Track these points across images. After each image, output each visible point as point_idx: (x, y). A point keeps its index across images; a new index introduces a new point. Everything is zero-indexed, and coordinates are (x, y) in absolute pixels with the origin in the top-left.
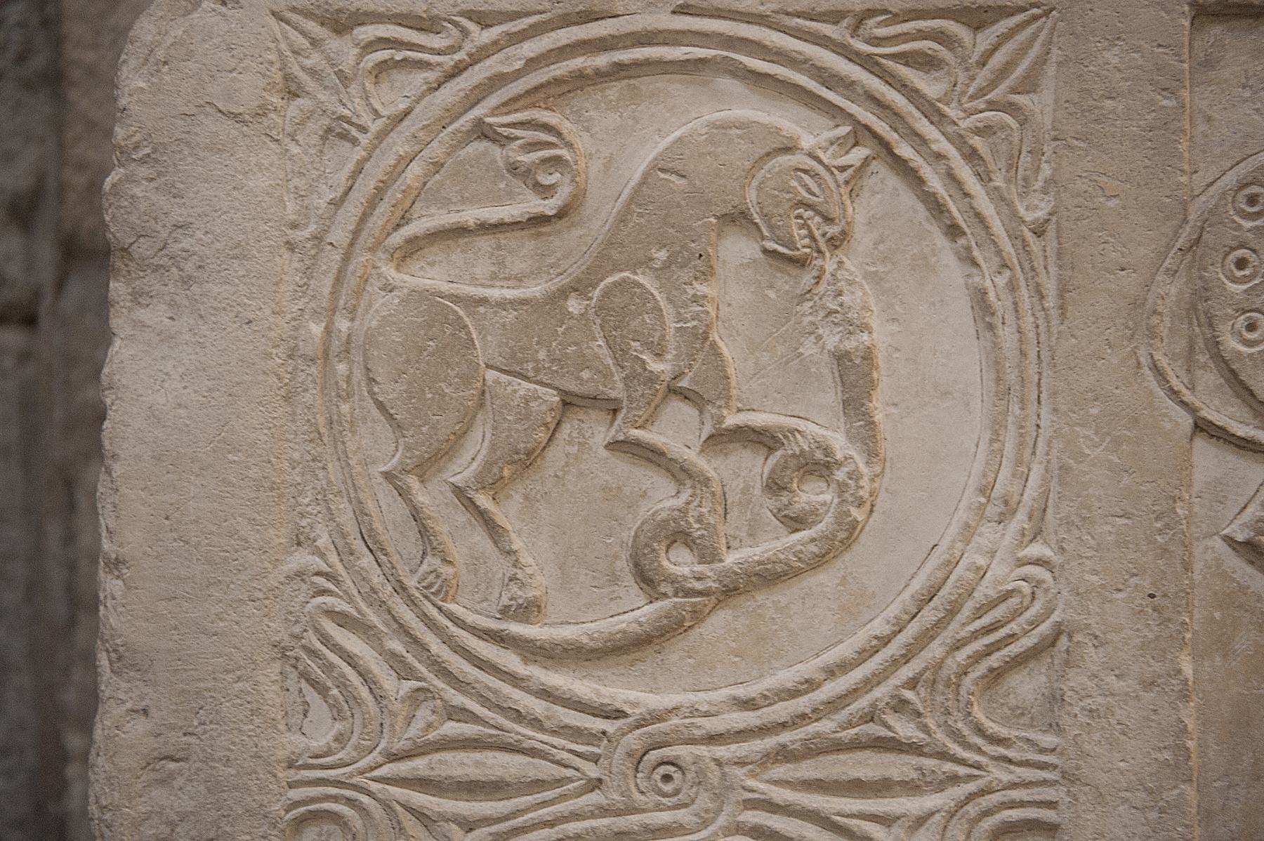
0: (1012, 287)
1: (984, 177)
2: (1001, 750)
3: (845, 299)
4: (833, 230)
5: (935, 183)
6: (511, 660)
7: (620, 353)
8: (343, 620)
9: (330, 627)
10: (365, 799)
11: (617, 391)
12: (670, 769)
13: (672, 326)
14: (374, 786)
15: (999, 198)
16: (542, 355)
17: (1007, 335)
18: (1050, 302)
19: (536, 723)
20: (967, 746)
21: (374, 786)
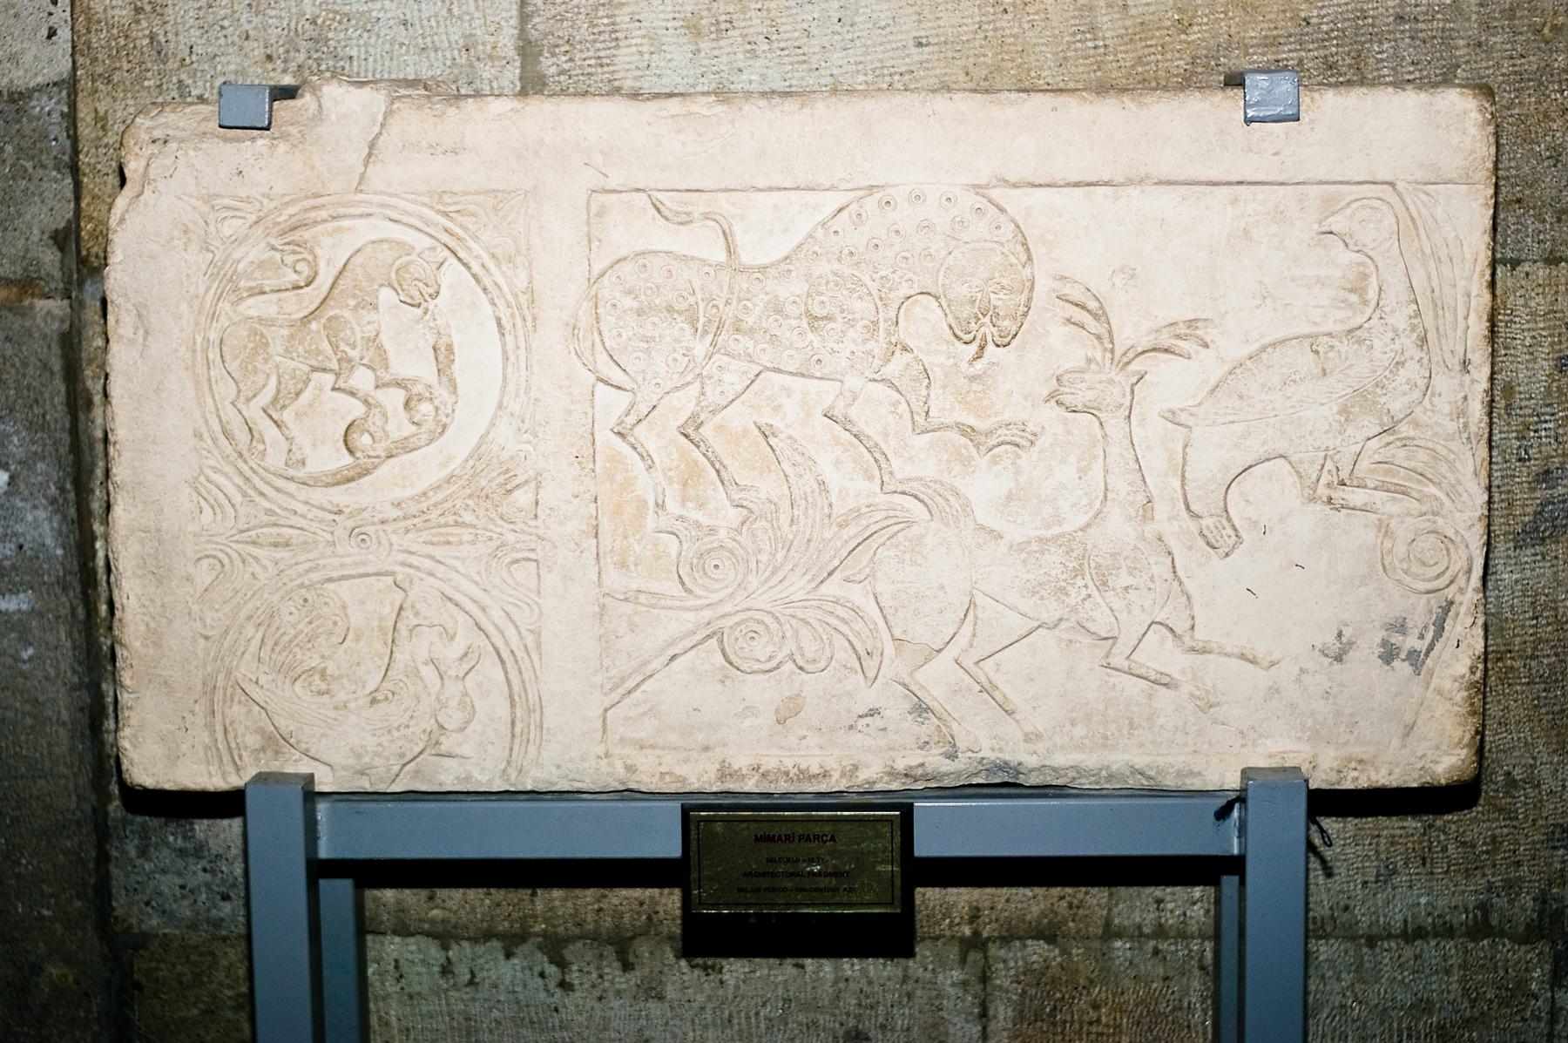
0: (512, 315)
1: (499, 266)
2: (511, 526)
3: (438, 322)
4: (431, 291)
5: (476, 268)
6: (292, 487)
7: (335, 348)
8: (215, 470)
9: (209, 472)
10: (229, 550)
11: (335, 366)
12: (364, 537)
13: (359, 335)
14: (233, 545)
15: (503, 273)
16: (300, 349)
17: (509, 338)
18: (529, 323)
19: (303, 516)
20: (496, 526)
21: (233, 545)
